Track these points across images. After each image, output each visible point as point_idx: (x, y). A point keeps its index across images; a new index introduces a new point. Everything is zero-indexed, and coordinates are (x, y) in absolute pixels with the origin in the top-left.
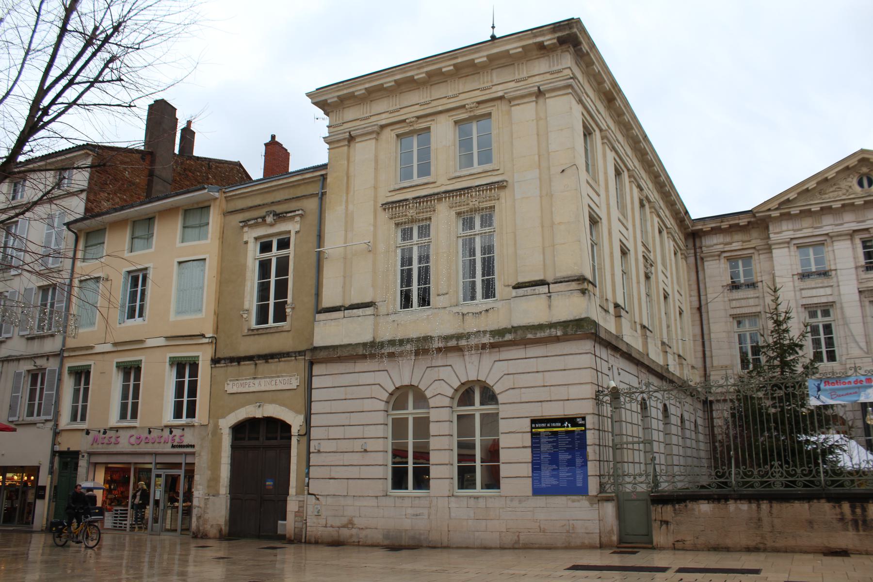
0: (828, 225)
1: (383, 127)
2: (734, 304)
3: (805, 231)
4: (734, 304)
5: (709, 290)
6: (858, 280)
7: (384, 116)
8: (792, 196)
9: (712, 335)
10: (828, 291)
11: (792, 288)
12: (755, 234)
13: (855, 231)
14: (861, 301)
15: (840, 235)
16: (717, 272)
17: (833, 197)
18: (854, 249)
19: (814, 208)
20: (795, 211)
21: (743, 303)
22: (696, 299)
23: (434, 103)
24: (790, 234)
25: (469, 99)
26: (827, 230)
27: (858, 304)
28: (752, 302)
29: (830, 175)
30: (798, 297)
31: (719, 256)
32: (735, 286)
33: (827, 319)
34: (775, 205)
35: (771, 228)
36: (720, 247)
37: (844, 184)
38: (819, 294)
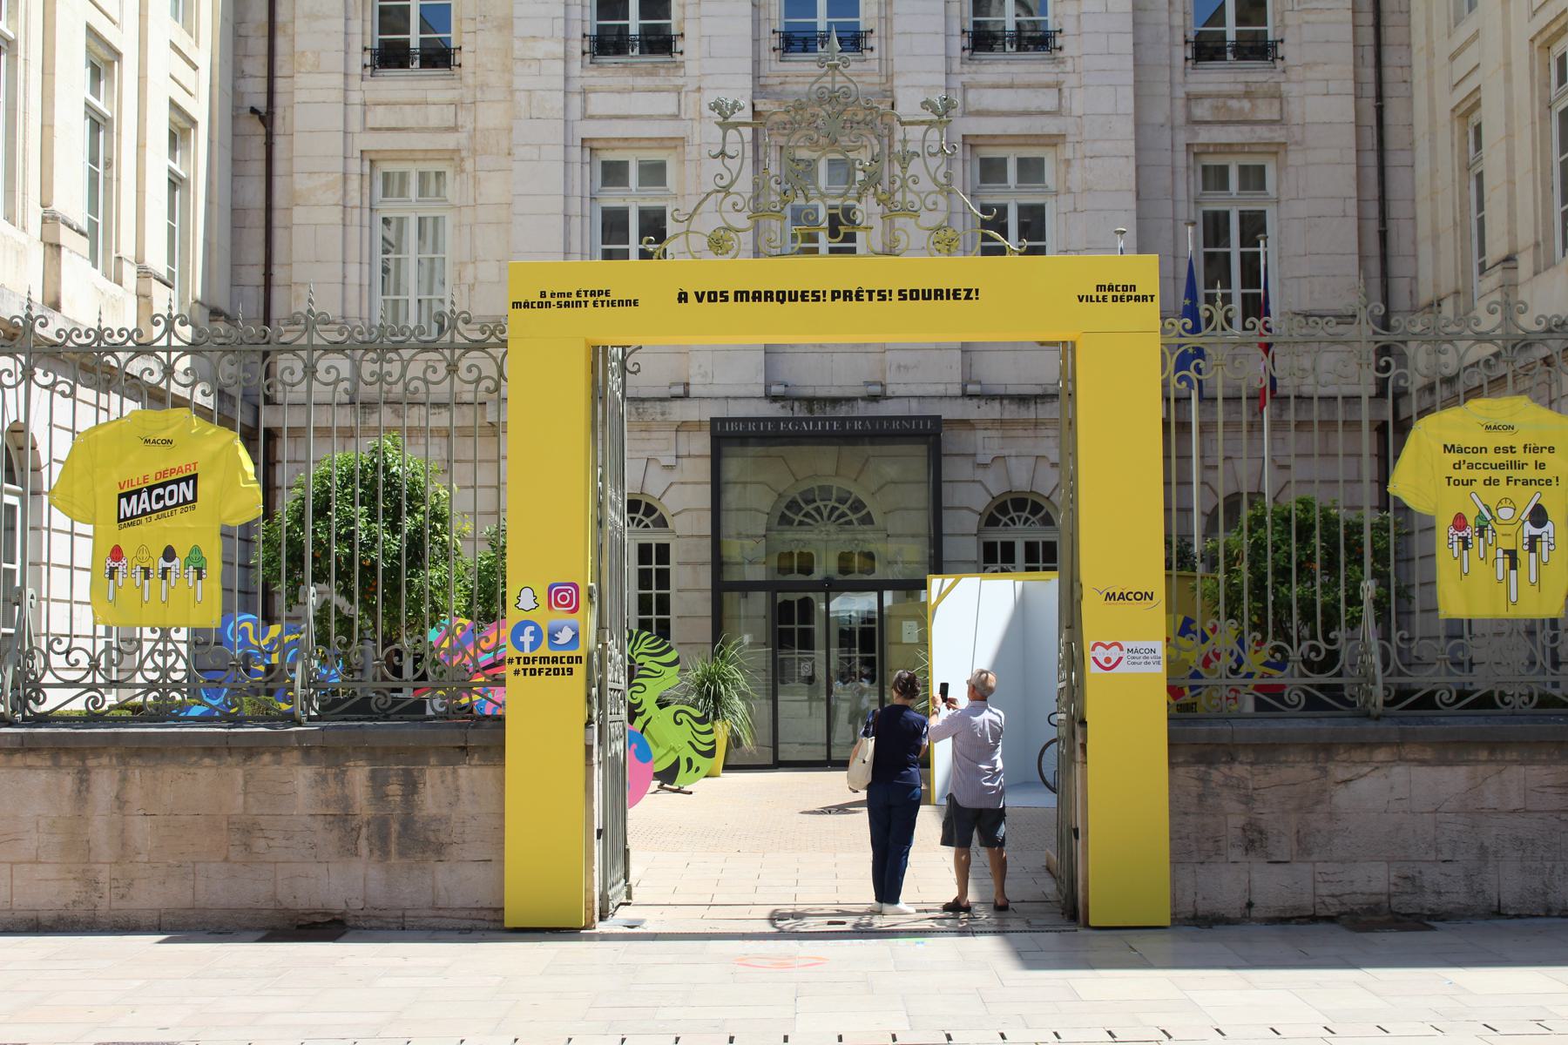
4: (379, 117)
6: (756, 77)
9: (299, 215)
10: (667, 104)
11: (560, 83)
28: (435, 116)
30: (576, 112)
32: (390, 56)
33: (652, 199)
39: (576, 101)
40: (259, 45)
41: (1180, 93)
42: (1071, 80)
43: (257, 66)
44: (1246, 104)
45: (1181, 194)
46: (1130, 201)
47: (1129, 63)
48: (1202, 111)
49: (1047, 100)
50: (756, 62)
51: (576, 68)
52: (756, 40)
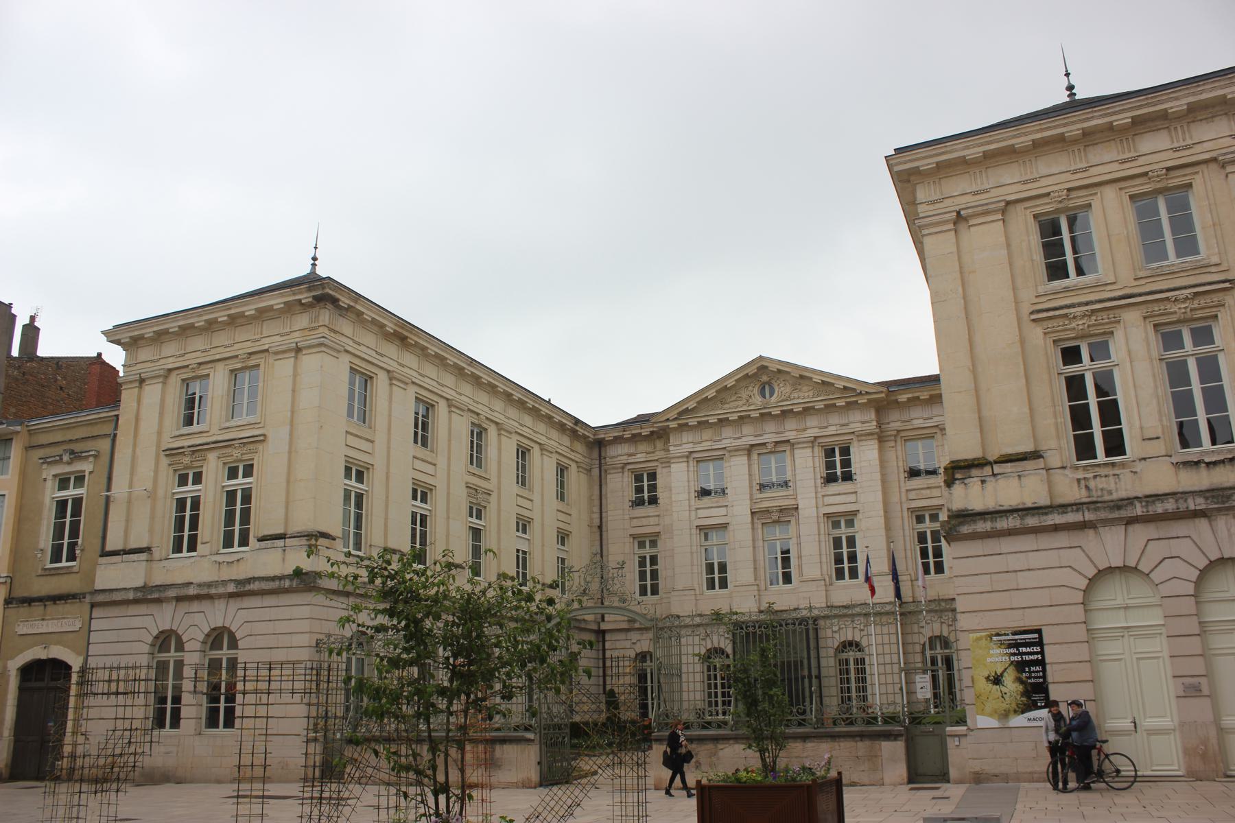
0: (728, 438)
1: (170, 370)
2: (635, 522)
3: (705, 444)
5: (610, 507)
6: (751, 499)
7: (171, 360)
8: (691, 405)
10: (723, 511)
12: (659, 444)
13: (752, 446)
14: (753, 523)
15: (736, 450)
16: (620, 487)
17: (732, 409)
18: (750, 465)
19: (713, 420)
20: (692, 422)
21: (645, 522)
22: (597, 516)
23: (213, 351)
24: (688, 448)
25: (241, 349)
26: (726, 443)
27: (750, 526)
28: (652, 521)
29: (730, 383)
31: (623, 468)
34: (673, 414)
35: (673, 439)
36: (624, 459)
37: (744, 394)
38: (711, 513)
39: (693, 513)
40: (597, 502)
41: (903, 490)
42: (859, 491)
43: (596, 509)
44: (928, 491)
45: (907, 527)
46: (883, 532)
47: (879, 483)
48: (912, 495)
49: (852, 498)
50: (751, 495)
51: (693, 502)
52: (751, 487)
